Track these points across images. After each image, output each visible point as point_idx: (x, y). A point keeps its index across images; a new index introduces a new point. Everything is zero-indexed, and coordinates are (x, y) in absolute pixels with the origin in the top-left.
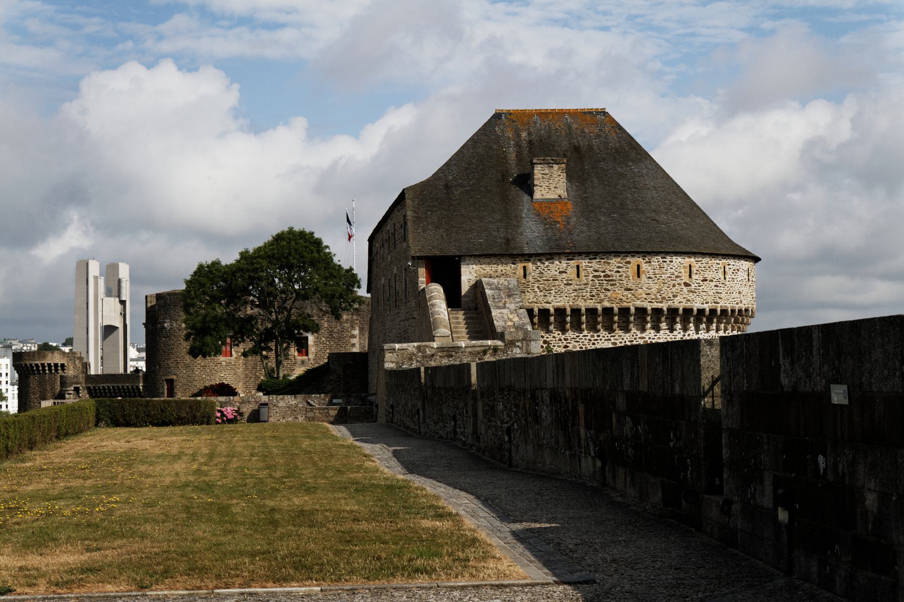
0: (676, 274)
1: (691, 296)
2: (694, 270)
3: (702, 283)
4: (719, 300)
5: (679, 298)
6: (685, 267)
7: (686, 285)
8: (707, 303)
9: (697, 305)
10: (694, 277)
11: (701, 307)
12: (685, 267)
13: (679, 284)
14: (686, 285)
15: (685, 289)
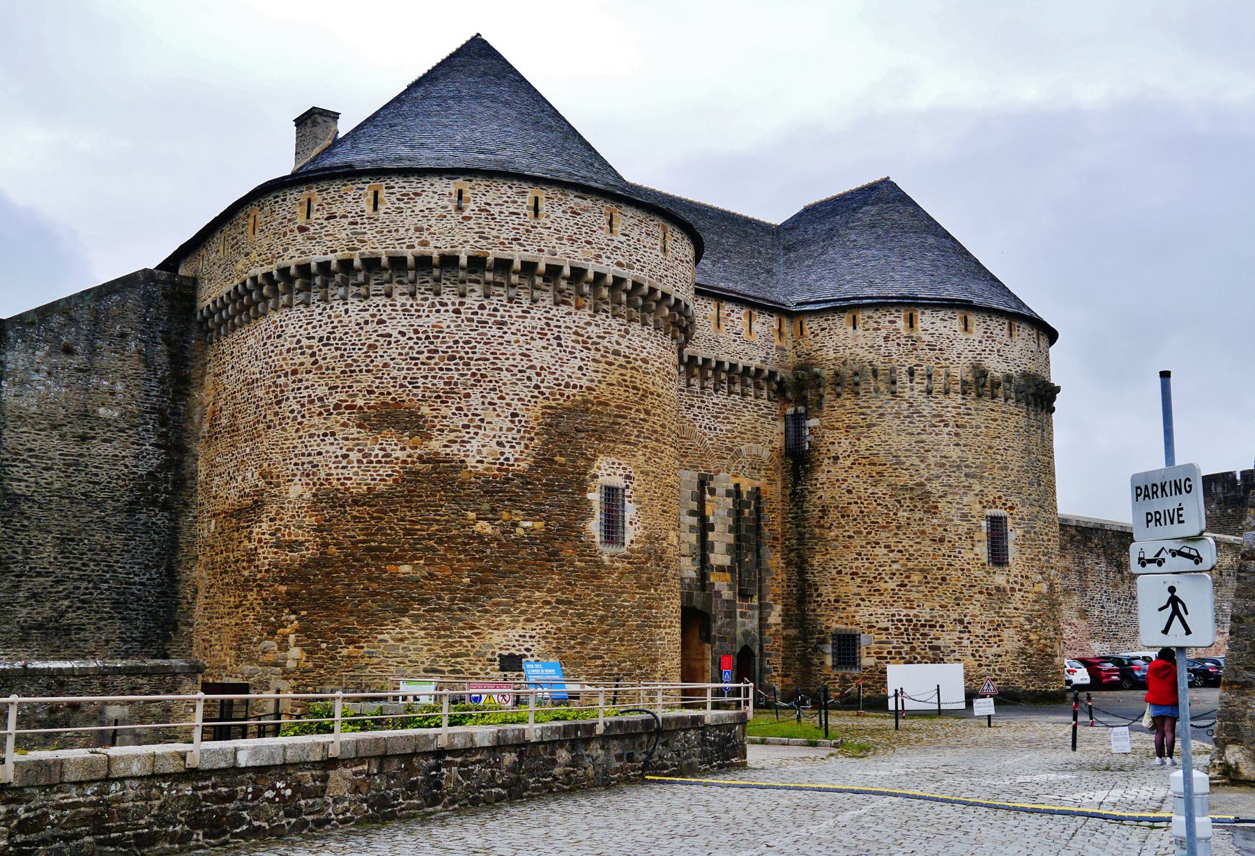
0: (288, 216)
1: (308, 245)
2: (315, 206)
3: (325, 223)
4: (358, 245)
5: (291, 252)
6: (301, 204)
7: (302, 229)
8: (334, 251)
9: (316, 258)
10: (313, 216)
11: (322, 258)
12: (301, 204)
13: (292, 231)
14: (302, 229)
15: (300, 238)
